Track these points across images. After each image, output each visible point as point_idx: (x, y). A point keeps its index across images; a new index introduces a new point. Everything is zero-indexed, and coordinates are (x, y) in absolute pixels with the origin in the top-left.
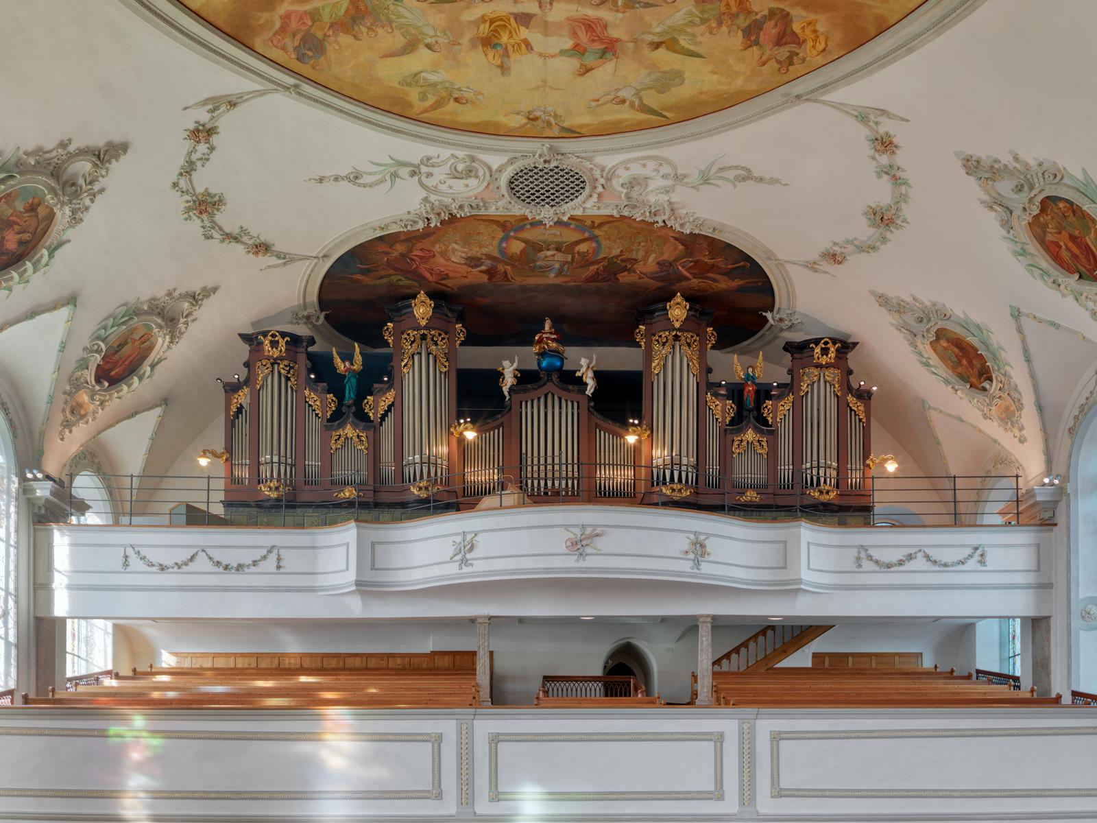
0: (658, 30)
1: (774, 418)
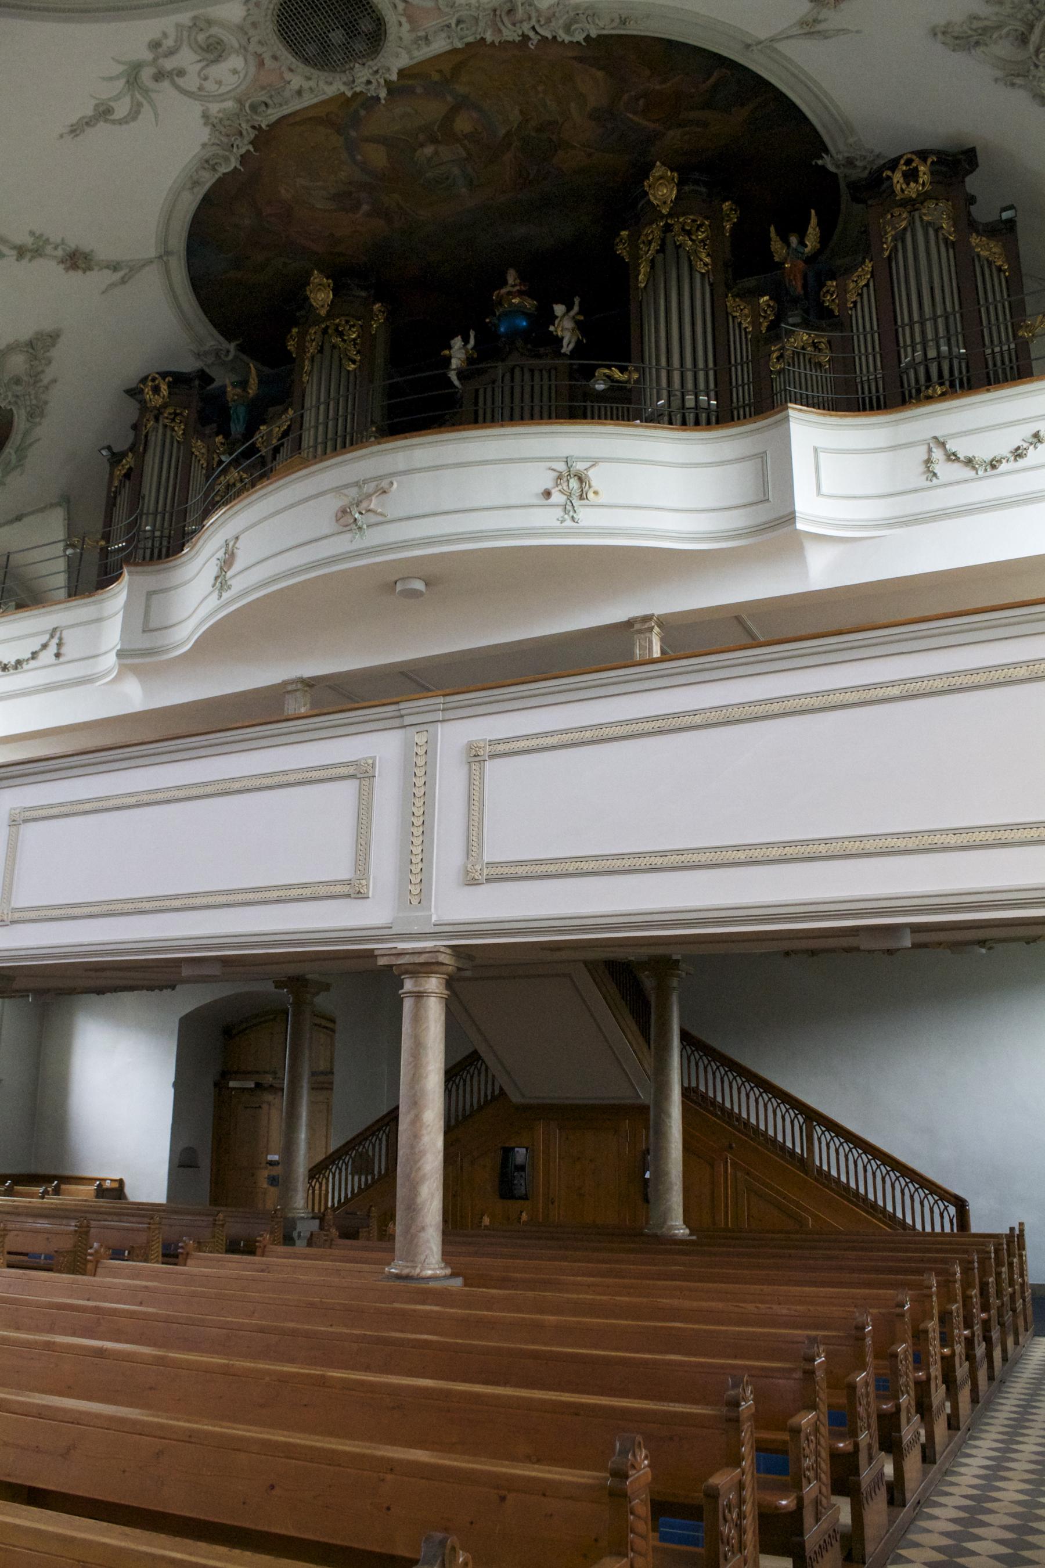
1: (843, 305)
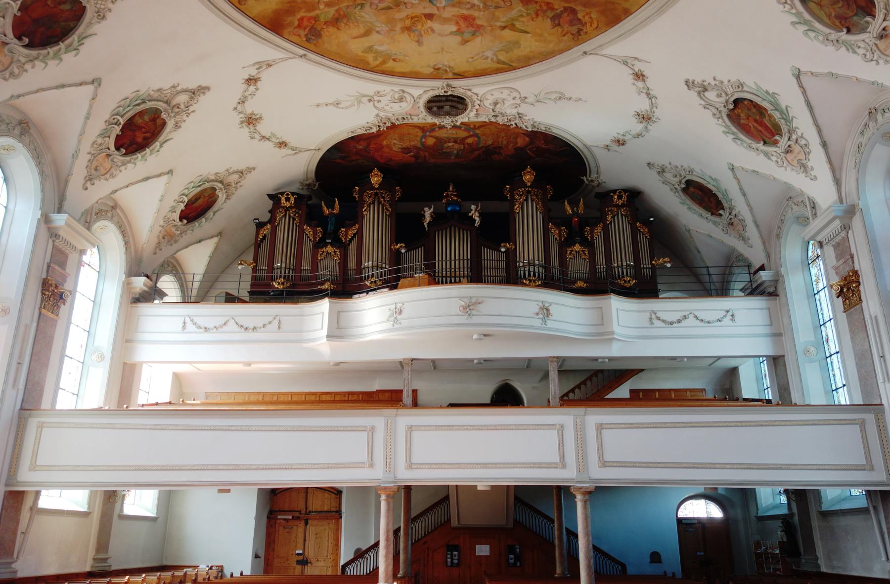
0: (504, 20)
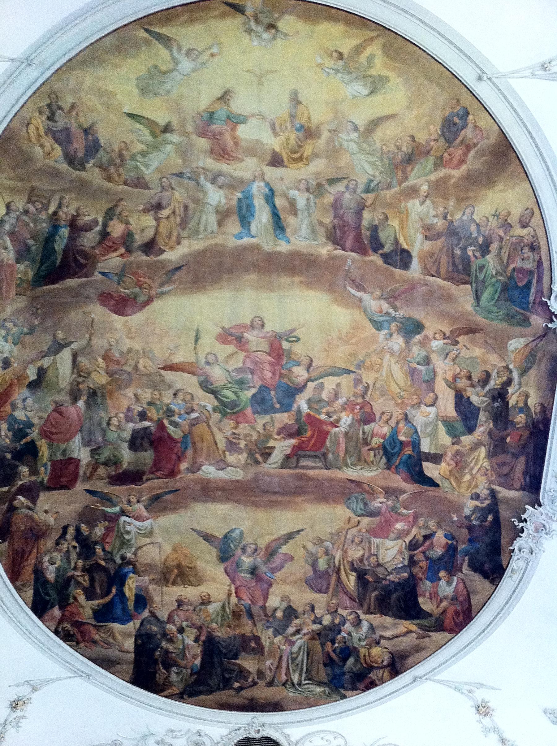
0: (169, 147)
